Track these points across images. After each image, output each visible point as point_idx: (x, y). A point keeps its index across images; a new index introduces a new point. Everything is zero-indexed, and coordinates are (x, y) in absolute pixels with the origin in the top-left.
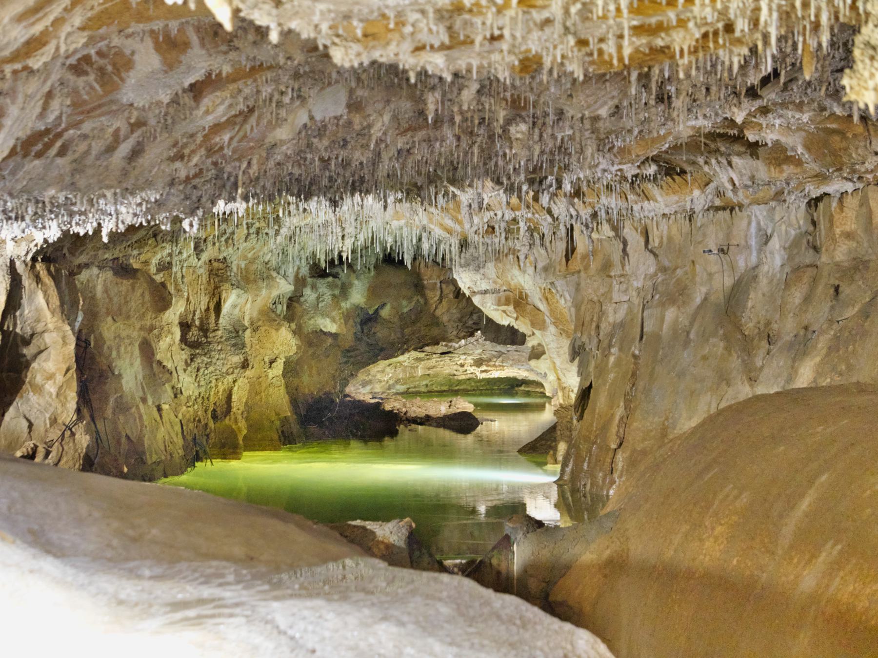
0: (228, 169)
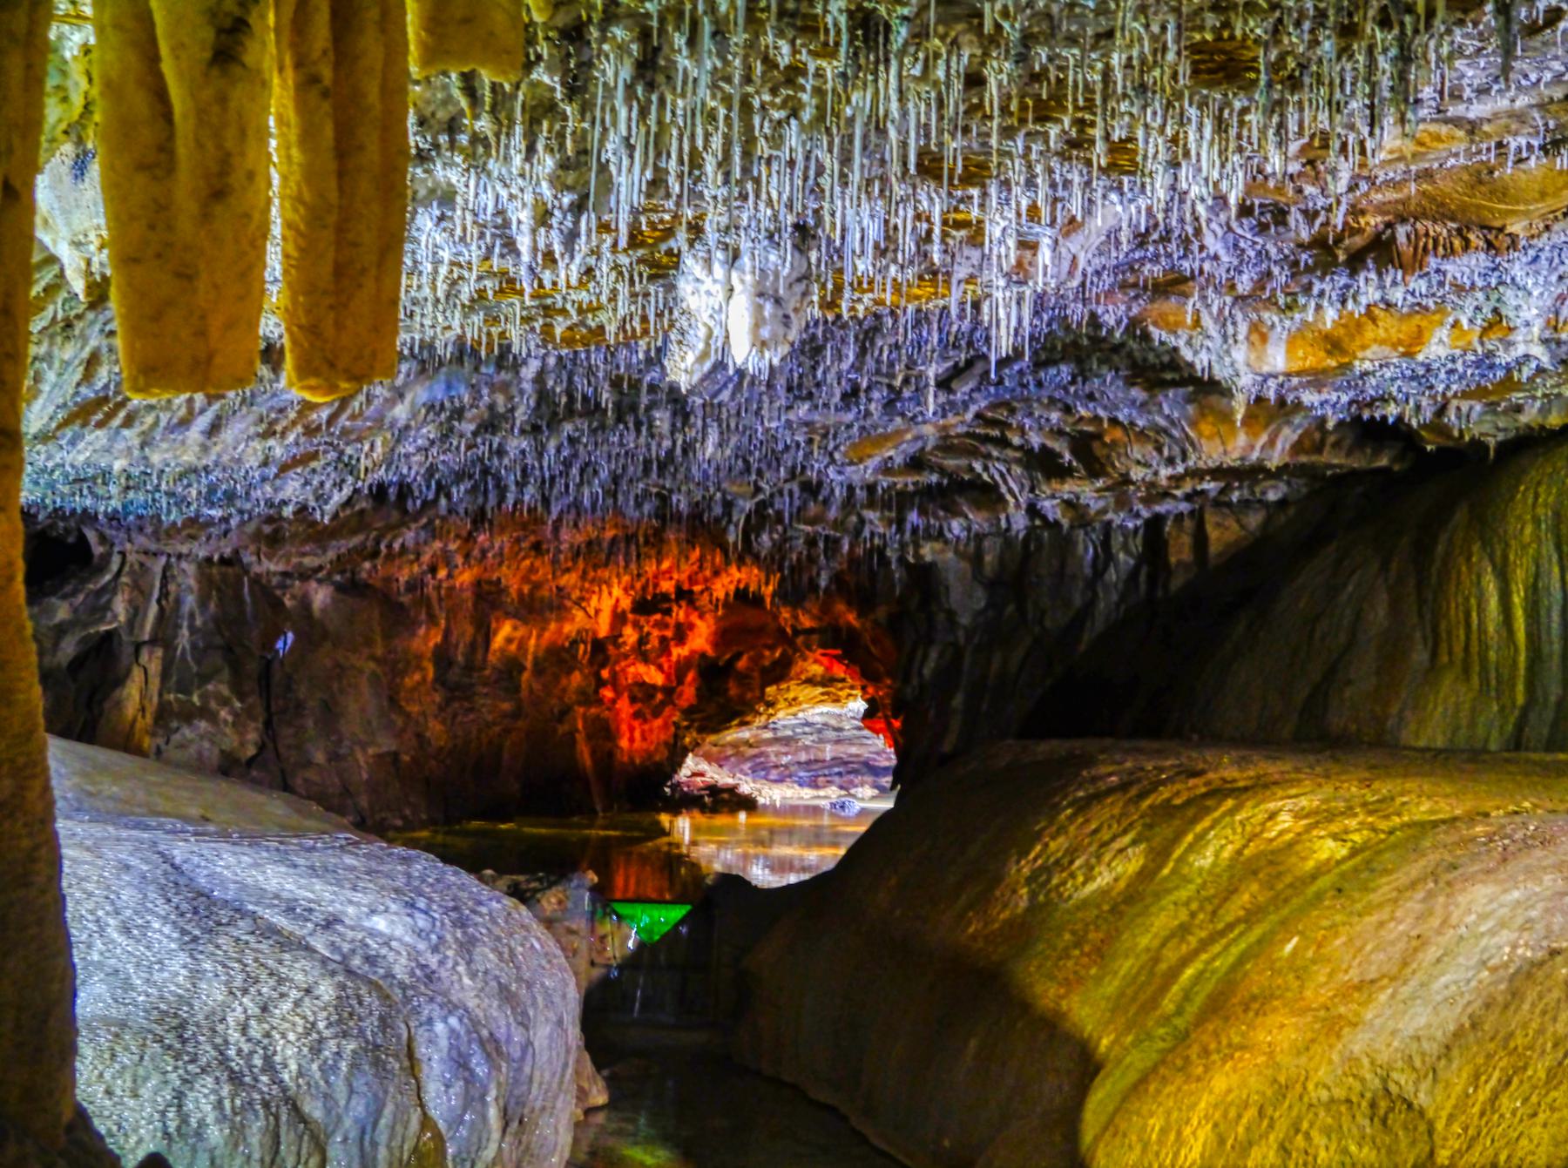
0: (349, 451)
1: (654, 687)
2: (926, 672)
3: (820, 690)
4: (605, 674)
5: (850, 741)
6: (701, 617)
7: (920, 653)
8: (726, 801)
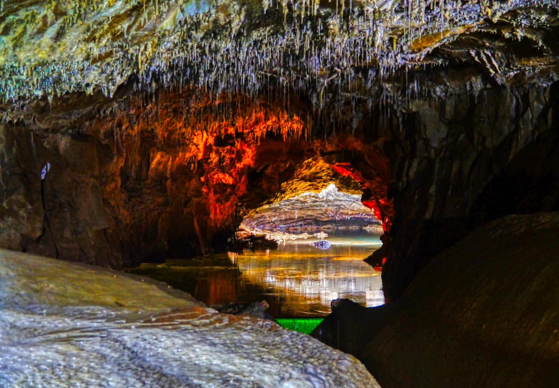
2: (411, 174)
3: (309, 183)
4: (202, 179)
5: (308, 209)
6: (248, 147)
7: (407, 164)
8: (260, 244)
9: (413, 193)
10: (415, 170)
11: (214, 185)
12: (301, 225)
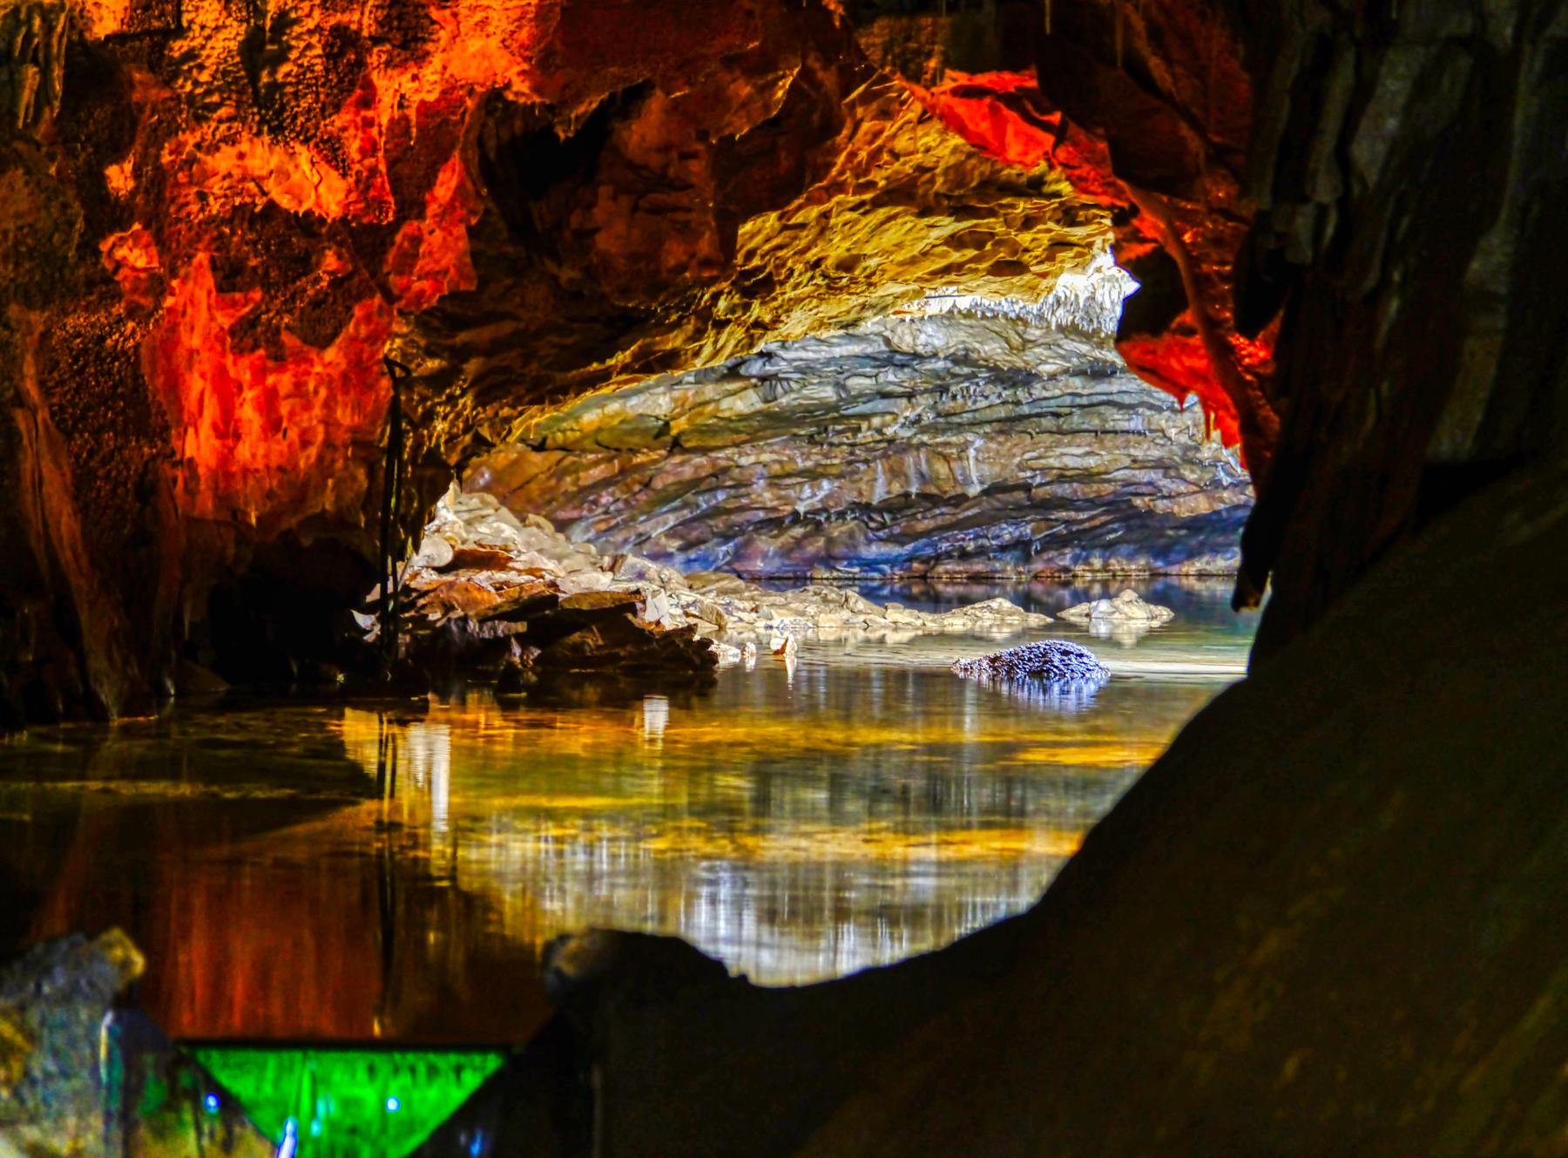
1: (308, 224)
2: (1367, 153)
3: (948, 226)
4: (119, 178)
7: (1341, 83)
8: (586, 659)
9: (1371, 282)
10: (1392, 124)
11: (211, 220)
12: (1021, 548)
